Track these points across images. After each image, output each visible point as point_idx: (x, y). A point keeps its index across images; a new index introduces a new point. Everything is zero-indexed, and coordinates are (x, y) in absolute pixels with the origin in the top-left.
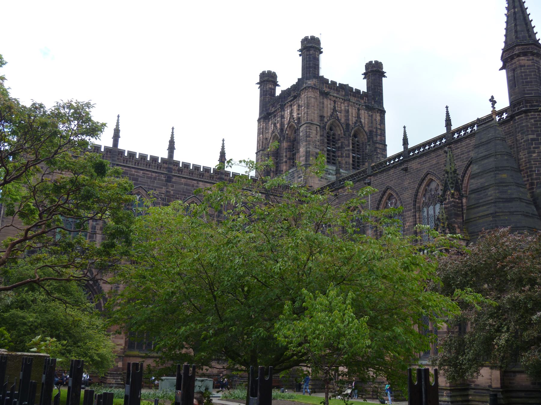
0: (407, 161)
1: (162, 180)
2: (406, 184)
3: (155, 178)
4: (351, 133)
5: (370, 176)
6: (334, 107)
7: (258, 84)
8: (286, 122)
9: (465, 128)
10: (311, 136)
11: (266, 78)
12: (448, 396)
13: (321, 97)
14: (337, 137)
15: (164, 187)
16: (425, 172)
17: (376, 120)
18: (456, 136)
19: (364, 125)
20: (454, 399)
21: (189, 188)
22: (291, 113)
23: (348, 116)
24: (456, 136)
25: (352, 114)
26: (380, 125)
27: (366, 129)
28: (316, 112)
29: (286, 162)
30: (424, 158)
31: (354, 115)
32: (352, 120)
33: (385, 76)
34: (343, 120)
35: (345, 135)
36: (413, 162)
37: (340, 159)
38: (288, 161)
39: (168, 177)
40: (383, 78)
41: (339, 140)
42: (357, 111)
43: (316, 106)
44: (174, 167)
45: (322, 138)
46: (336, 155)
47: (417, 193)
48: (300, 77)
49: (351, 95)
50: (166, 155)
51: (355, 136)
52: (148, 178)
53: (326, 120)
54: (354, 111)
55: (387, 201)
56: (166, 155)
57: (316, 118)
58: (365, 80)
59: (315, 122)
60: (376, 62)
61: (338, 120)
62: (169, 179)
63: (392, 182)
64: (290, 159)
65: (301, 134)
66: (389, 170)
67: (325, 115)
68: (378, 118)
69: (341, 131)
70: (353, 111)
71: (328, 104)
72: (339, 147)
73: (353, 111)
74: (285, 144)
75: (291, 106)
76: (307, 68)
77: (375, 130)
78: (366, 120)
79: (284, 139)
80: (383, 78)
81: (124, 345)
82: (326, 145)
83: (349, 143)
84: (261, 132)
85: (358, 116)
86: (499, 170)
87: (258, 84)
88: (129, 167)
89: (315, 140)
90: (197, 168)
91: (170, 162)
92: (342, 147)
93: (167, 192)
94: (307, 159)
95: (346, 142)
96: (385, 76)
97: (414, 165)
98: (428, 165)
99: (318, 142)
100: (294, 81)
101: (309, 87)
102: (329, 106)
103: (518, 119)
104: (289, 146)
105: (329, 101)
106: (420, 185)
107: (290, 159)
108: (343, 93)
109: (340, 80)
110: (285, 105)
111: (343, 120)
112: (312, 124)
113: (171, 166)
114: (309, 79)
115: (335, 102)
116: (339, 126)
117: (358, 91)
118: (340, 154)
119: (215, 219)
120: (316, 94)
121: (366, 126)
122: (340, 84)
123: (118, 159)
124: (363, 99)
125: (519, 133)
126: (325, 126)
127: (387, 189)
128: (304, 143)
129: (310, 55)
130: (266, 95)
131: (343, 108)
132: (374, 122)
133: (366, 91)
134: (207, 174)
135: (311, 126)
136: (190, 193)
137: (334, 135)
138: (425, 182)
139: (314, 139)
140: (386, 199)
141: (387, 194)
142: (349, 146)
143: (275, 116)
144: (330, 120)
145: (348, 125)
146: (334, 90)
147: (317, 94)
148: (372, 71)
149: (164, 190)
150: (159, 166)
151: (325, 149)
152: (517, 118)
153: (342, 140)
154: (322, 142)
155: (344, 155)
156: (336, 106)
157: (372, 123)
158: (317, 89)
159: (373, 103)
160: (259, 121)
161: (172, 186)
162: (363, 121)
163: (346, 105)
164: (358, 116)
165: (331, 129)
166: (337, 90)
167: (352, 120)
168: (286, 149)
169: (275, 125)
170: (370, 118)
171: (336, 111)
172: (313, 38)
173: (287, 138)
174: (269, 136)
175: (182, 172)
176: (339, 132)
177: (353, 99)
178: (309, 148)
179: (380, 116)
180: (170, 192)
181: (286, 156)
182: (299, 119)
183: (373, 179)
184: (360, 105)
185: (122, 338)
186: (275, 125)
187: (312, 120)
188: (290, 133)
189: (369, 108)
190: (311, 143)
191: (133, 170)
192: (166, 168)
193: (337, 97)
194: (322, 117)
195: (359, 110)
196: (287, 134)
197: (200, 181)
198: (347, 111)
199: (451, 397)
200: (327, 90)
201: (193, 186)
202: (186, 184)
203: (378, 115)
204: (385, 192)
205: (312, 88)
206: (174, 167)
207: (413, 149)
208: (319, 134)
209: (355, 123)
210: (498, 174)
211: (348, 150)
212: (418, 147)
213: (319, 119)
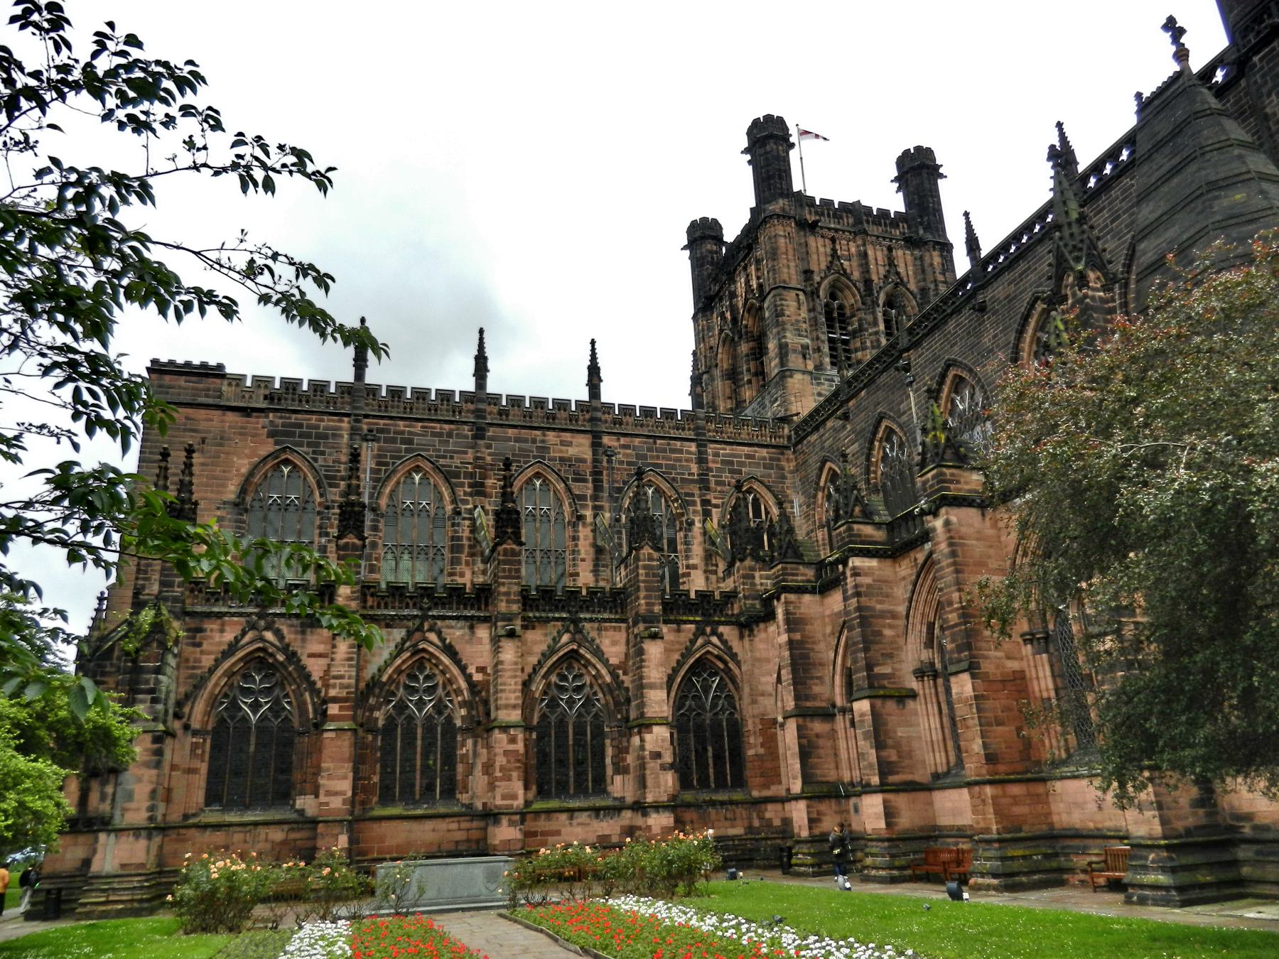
0: (983, 287)
1: (466, 437)
2: (986, 341)
3: (450, 435)
4: (877, 298)
5: (907, 350)
6: (834, 250)
7: (684, 248)
8: (740, 305)
9: (1112, 154)
10: (787, 313)
11: (698, 234)
12: (1164, 870)
13: (802, 233)
14: (848, 312)
15: (470, 451)
16: (1027, 297)
17: (932, 265)
18: (1092, 182)
19: (905, 279)
20: (1185, 878)
21: (524, 445)
22: (747, 282)
23: (867, 264)
24: (1092, 182)
26: (943, 274)
27: (912, 286)
28: (792, 264)
29: (749, 382)
30: (1022, 266)
31: (880, 262)
32: (877, 271)
33: (942, 176)
34: (856, 275)
35: (863, 303)
36: (995, 285)
37: (859, 354)
38: (754, 380)
39: (478, 429)
40: (940, 182)
41: (853, 316)
42: (886, 252)
43: (791, 252)
44: (489, 409)
45: (812, 315)
46: (852, 346)
47: (1017, 353)
48: (754, 205)
49: (868, 222)
50: (470, 385)
51: (890, 303)
52: (434, 435)
53: (817, 279)
54: (879, 254)
55: (953, 395)
56: (470, 385)
57: (794, 277)
58: (901, 194)
59: (793, 284)
60: (918, 149)
61: (845, 274)
62: (479, 433)
63: (956, 348)
64: (756, 374)
65: (767, 314)
66: (946, 323)
67: (814, 267)
68: (937, 260)
69: (854, 296)
70: (876, 255)
71: (819, 248)
72: (855, 332)
73: (876, 255)
74: (744, 348)
75: (745, 268)
76: (763, 180)
77: (932, 286)
78: (910, 268)
79: (740, 338)
80: (940, 182)
81: (349, 793)
82: (825, 329)
83: (875, 319)
84: (700, 337)
85: (891, 262)
86: (1220, 188)
87: (684, 248)
88: (391, 418)
89: (797, 321)
90: (539, 403)
91: (479, 397)
92: (861, 329)
93: (478, 458)
94: (782, 364)
95: (870, 318)
96: (942, 176)
97: (998, 291)
98: (1032, 277)
100: (745, 218)
101: (771, 217)
102: (822, 249)
103: (1261, 60)
104: (752, 349)
105: (820, 241)
106: (1021, 332)
107: (756, 374)
108: (851, 221)
109: (839, 196)
110: (735, 270)
111: (856, 275)
112: (785, 288)
113: (481, 406)
114: (769, 202)
115: (833, 240)
116: (848, 287)
117: (884, 213)
118: (858, 344)
119: (590, 503)
120: (788, 229)
121: (912, 280)
122: (840, 203)
123: (367, 405)
124: (898, 226)
125: (1269, 95)
126: (818, 290)
127: (948, 367)
128: (775, 331)
129: (766, 153)
130: (702, 265)
131: (853, 250)
132: (929, 270)
133: (903, 210)
134: (563, 414)
135: (785, 293)
136: (528, 456)
137: (841, 307)
138: (1032, 322)
139: (793, 319)
140: (950, 392)
141: (948, 381)
142: (875, 323)
143: (721, 299)
144: (826, 277)
145: (868, 282)
146: (829, 215)
147: (792, 227)
148: (912, 168)
149: (470, 456)
150: (456, 409)
151: (824, 337)
152: (1256, 59)
153: (861, 315)
154: (814, 323)
155: (868, 344)
156: (838, 247)
157: (923, 271)
158: (789, 218)
159: (921, 232)
160: (695, 318)
161: (489, 447)
162: (901, 270)
163: (859, 242)
164: (891, 262)
165: (833, 296)
166: (835, 216)
167: (877, 271)
168: (747, 355)
169: (722, 315)
170: (918, 263)
171: (839, 258)
172: (769, 118)
173: (747, 333)
174: (713, 342)
175: (507, 415)
176: (851, 299)
177: (873, 230)
178: (785, 337)
179: (941, 256)
180: (483, 459)
181: (748, 370)
182: (760, 286)
183: (912, 354)
184: (891, 240)
185: (345, 778)
186: (722, 315)
187: (784, 282)
188: (750, 323)
189: (912, 243)
190: (788, 326)
191: (401, 423)
192: (473, 412)
193: (836, 230)
194: (808, 273)
195: (890, 249)
196: (746, 326)
197: (549, 429)
198: (864, 255)
199: (1173, 870)
200: (811, 218)
201: (534, 441)
202: (517, 440)
203: (936, 254)
204: (943, 376)
205: (778, 216)
206: (489, 409)
207: (994, 255)
208: (804, 308)
209: (886, 277)
210: (1217, 198)
211: (877, 333)
212: (1003, 247)
213: (802, 278)
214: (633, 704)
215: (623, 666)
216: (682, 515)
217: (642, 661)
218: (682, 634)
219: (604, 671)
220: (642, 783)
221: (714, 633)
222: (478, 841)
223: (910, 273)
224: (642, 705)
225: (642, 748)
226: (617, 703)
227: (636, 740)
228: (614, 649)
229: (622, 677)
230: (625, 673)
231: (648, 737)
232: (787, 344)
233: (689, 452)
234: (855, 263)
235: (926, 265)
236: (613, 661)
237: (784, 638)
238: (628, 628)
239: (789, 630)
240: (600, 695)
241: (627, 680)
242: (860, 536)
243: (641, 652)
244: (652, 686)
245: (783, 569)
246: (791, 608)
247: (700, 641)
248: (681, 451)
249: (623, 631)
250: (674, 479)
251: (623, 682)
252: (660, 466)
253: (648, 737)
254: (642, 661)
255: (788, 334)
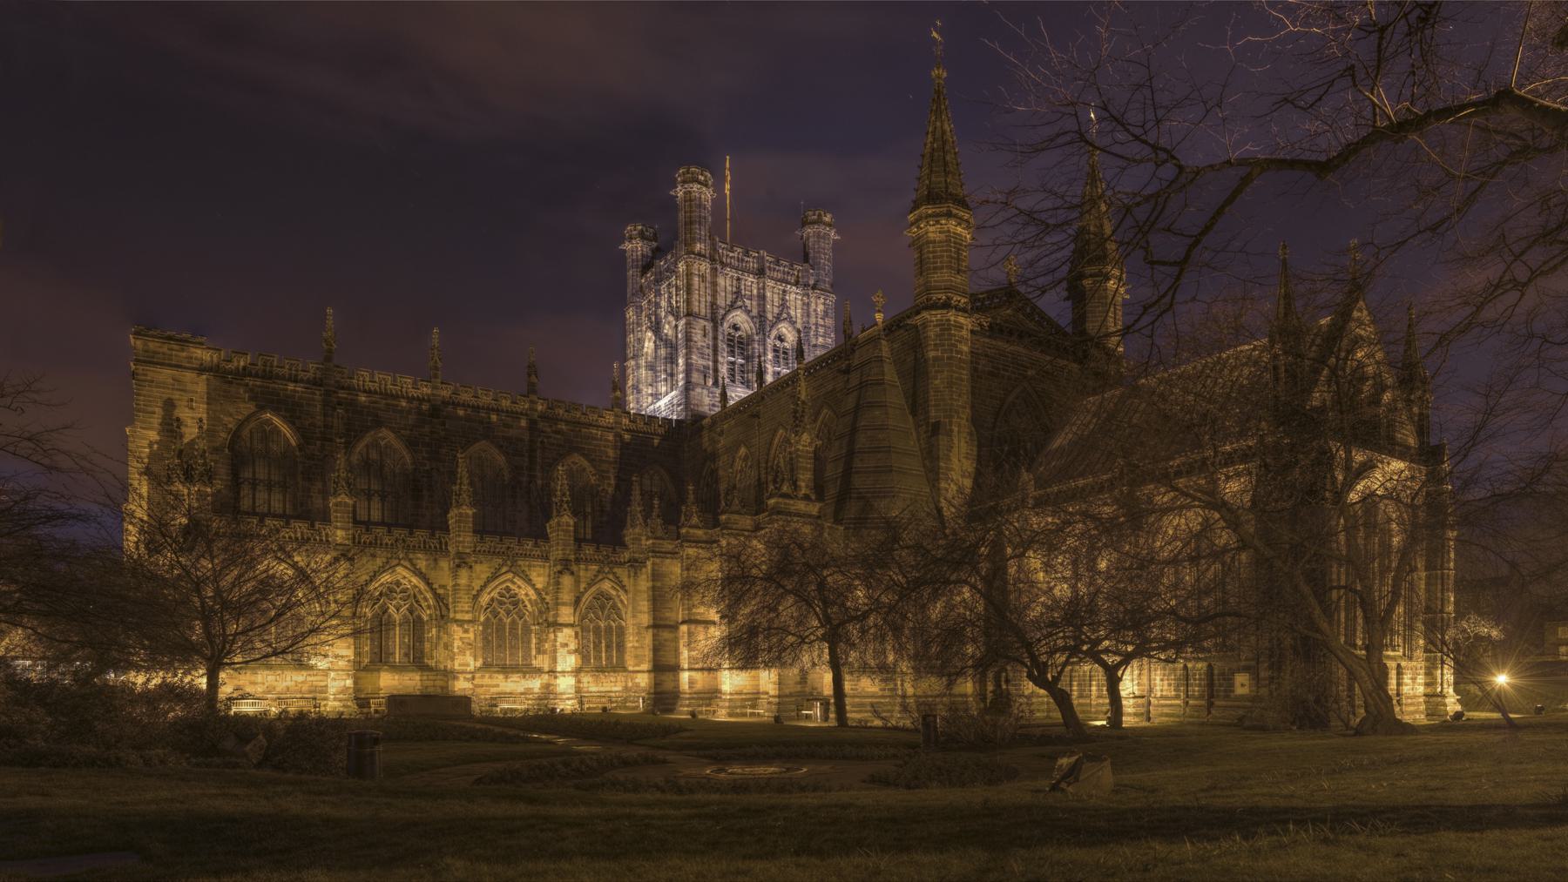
17: (815, 310)
22: (670, 298)
23: (764, 305)
25: (773, 301)
74: (662, 352)
77: (813, 327)
99: (708, 348)
102: (729, 288)
111: (755, 312)
121: (799, 321)
156: (743, 287)
162: (792, 313)
164: (784, 305)
168: (666, 358)
171: (743, 297)
178: (691, 358)
198: (762, 297)
214: (552, 613)
215: (545, 589)
216: (599, 486)
217: (558, 589)
218: (589, 572)
219: (531, 592)
220: (554, 660)
221: (608, 572)
222: (442, 688)
223: (799, 315)
224: (556, 615)
225: (555, 640)
226: (541, 612)
227: (552, 636)
228: (541, 579)
229: (544, 596)
230: (547, 594)
231: (559, 634)
232: (692, 364)
233: (608, 441)
234: (755, 303)
235: (811, 310)
236: (539, 586)
237: (650, 584)
238: (550, 567)
239: (653, 581)
240: (529, 606)
241: (548, 598)
242: (693, 537)
243: (558, 583)
244: (564, 604)
245: (653, 543)
246: (656, 568)
247: (600, 577)
248: (601, 440)
249: (547, 568)
250: (593, 460)
251: (544, 599)
252: (584, 449)
253: (559, 634)
254: (558, 589)
255: (694, 357)
